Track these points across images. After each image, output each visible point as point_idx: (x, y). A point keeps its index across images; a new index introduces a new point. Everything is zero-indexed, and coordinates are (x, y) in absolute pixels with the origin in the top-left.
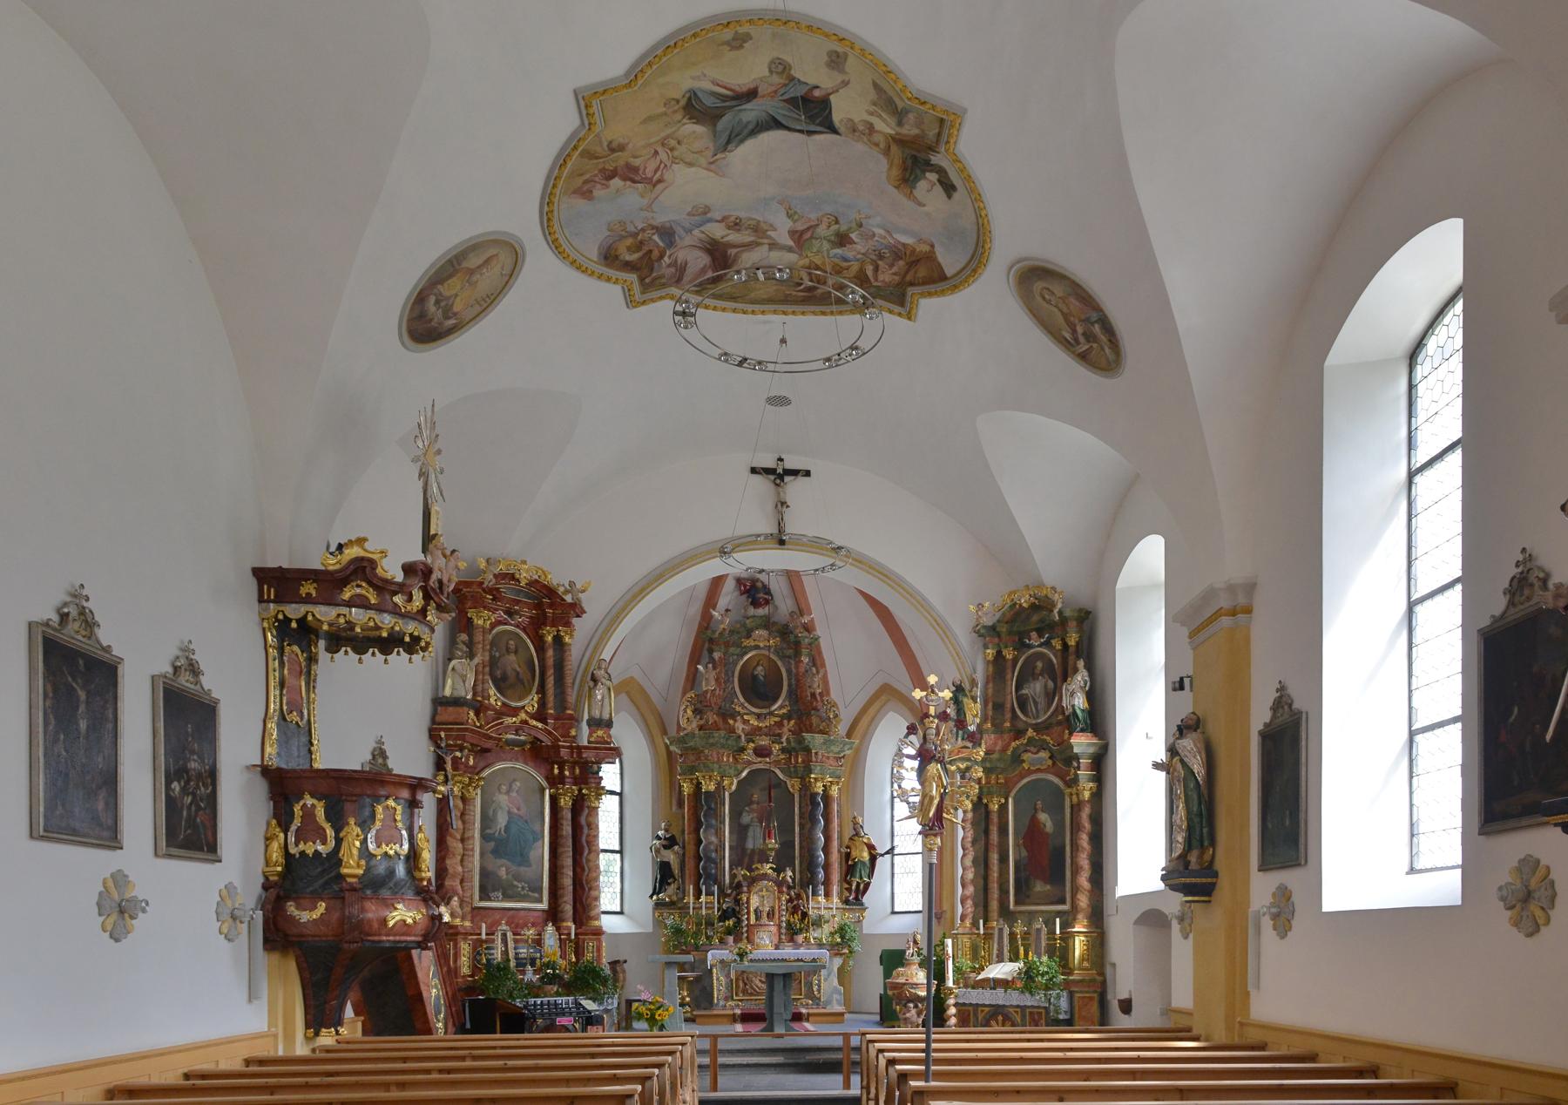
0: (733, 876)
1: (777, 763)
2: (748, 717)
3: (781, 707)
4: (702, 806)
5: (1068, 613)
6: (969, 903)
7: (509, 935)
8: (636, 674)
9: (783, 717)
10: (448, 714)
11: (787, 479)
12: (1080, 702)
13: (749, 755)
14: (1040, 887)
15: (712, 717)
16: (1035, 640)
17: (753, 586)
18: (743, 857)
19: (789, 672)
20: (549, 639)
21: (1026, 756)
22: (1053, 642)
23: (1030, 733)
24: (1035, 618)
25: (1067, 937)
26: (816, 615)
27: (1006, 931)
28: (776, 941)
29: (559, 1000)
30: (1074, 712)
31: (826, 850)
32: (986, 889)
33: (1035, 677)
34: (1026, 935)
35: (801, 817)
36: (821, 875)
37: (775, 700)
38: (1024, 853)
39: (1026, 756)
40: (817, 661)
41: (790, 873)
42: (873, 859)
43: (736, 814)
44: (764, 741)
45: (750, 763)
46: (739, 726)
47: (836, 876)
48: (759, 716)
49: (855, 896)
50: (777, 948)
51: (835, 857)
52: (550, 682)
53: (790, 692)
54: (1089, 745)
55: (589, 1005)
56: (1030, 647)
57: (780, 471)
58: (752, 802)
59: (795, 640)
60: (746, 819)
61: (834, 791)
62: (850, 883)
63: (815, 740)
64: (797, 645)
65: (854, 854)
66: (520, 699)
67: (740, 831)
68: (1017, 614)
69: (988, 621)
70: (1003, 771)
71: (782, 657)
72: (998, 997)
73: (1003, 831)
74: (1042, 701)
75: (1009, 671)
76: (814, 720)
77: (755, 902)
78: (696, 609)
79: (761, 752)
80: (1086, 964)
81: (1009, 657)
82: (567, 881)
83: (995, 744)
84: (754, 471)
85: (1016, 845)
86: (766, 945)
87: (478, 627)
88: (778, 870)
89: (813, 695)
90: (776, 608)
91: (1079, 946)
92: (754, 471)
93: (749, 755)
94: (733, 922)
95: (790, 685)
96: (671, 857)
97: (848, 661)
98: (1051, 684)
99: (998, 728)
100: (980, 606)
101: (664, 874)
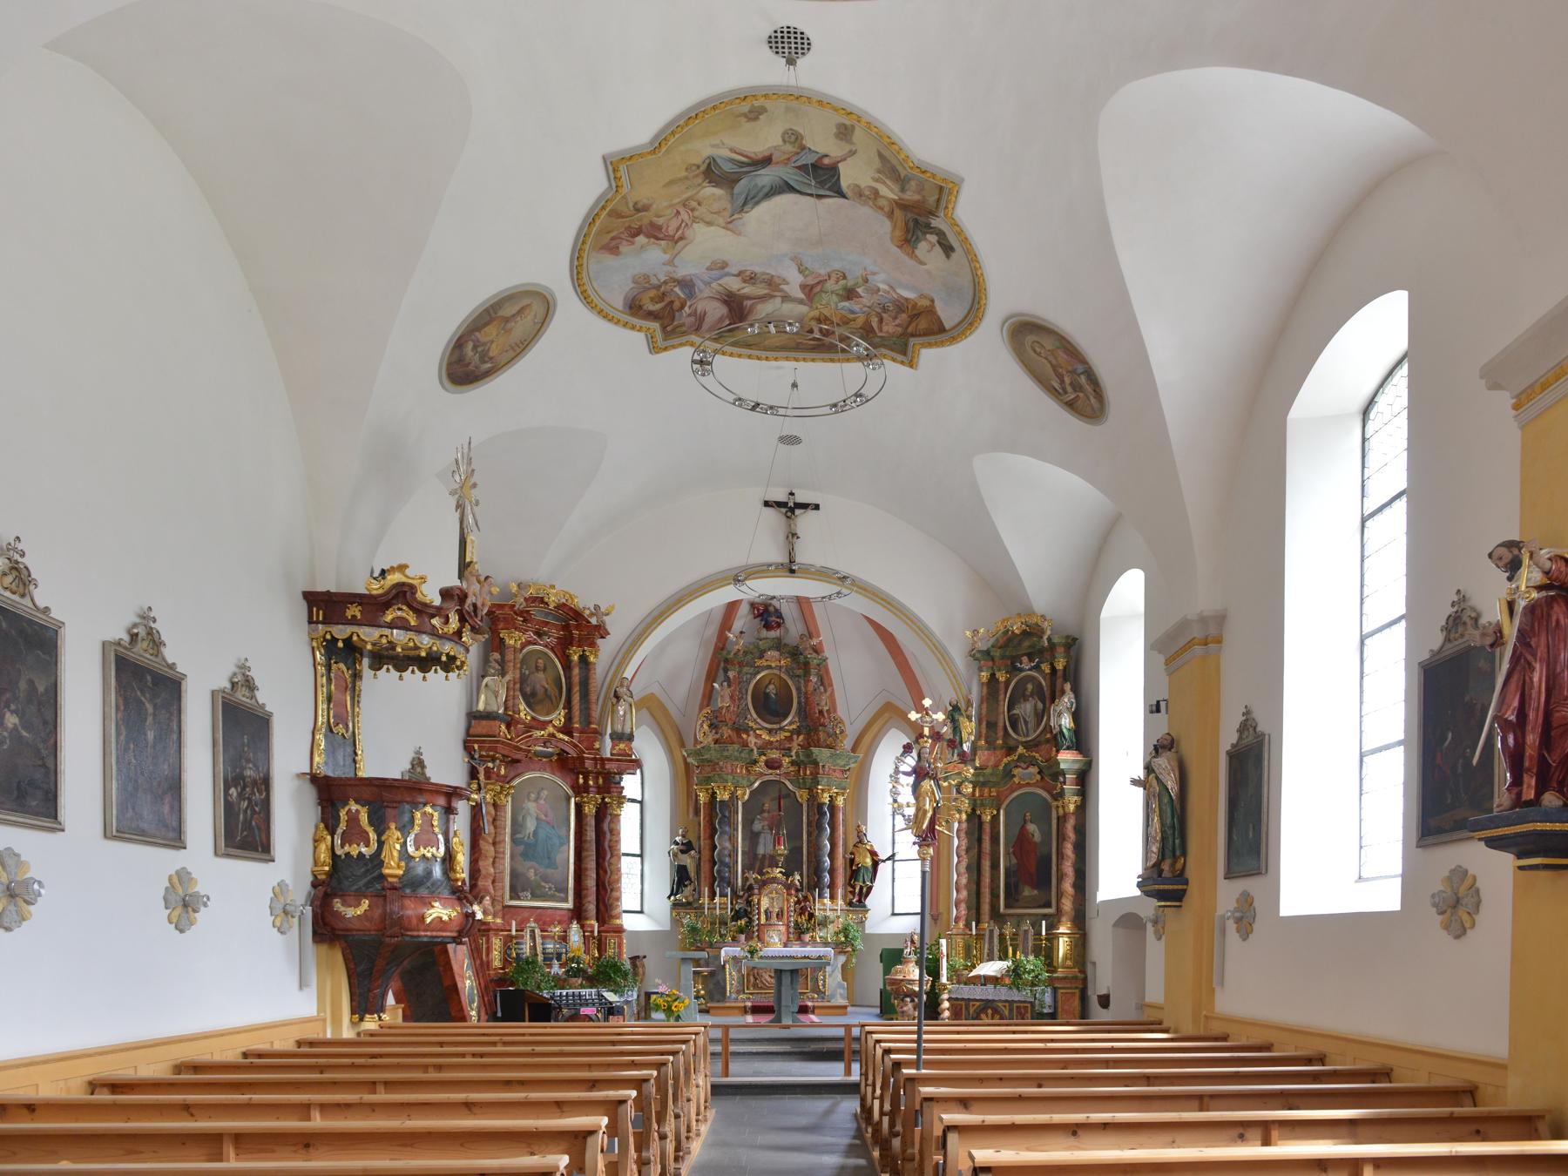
5: (1056, 640)
6: (963, 906)
12: (1066, 722)
14: (1027, 892)
16: (1025, 663)
21: (1016, 771)
23: (1021, 750)
25: (1052, 938)
27: (996, 932)
28: (784, 939)
30: (1061, 732)
31: (832, 855)
32: (978, 893)
34: (1014, 936)
36: (827, 879)
38: (1014, 861)
39: (1016, 771)
42: (875, 864)
47: (840, 880)
49: (858, 899)
50: (785, 946)
51: (840, 862)
52: (576, 698)
66: (548, 714)
68: (1010, 640)
70: (996, 784)
72: (989, 993)
74: (1032, 721)
77: (765, 903)
80: (1069, 963)
81: (1002, 679)
82: (591, 882)
85: (1007, 853)
88: (787, 874)
91: (1063, 946)
98: (1040, 705)
99: (991, 744)
100: (975, 632)
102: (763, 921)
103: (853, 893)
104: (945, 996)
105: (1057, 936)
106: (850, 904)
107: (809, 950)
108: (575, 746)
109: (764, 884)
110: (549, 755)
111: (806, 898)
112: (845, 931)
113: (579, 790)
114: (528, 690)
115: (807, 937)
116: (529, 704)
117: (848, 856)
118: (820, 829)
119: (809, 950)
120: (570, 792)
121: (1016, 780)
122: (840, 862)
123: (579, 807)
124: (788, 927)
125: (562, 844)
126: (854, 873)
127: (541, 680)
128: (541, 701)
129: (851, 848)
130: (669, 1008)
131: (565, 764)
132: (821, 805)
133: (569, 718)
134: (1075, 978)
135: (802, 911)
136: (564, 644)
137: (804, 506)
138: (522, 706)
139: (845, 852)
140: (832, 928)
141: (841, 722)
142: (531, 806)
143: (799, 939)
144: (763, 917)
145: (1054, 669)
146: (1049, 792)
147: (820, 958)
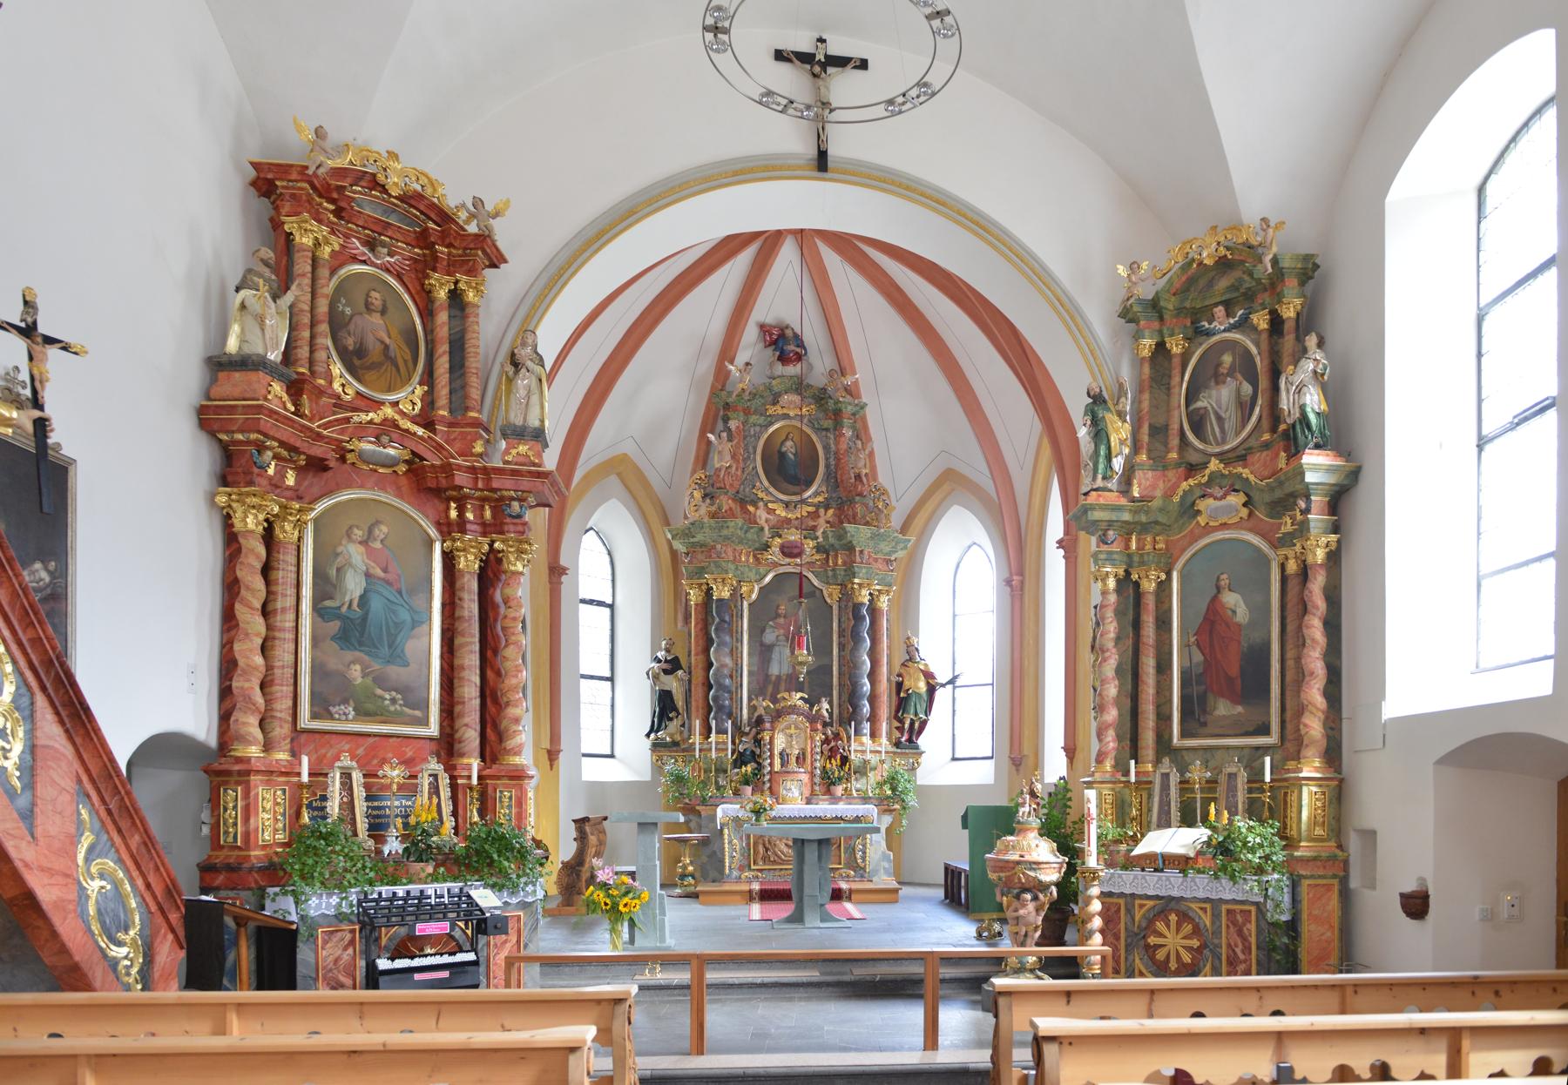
0: (752, 709)
1: (811, 564)
2: (772, 507)
3: (816, 494)
4: (711, 619)
5: (1286, 263)
6: (1110, 735)
7: (357, 777)
8: (629, 448)
9: (817, 506)
10: (237, 381)
11: (830, 70)
12: (1313, 400)
13: (774, 554)
14: (1223, 709)
15: (726, 503)
16: (1220, 322)
17: (782, 336)
18: (765, 685)
19: (826, 448)
20: (442, 294)
21: (1202, 505)
22: (1255, 318)
23: (1214, 465)
24: (1223, 283)
26: (861, 375)
27: (1174, 779)
28: (807, 793)
29: (430, 889)
30: (1304, 419)
31: (872, 676)
32: (1135, 713)
33: (1218, 379)
35: (840, 635)
36: (866, 709)
37: (809, 484)
38: (1198, 657)
40: (862, 434)
41: (826, 706)
42: (931, 690)
43: (757, 631)
44: (793, 536)
45: (776, 565)
46: (762, 515)
48: (787, 505)
49: (908, 737)
50: (808, 802)
51: (884, 686)
52: (443, 364)
53: (828, 475)
54: (1330, 470)
55: (486, 898)
56: (1209, 334)
57: (820, 57)
58: (778, 616)
59: (834, 407)
60: (769, 637)
61: (883, 603)
62: (901, 721)
63: (859, 534)
64: (837, 414)
65: (907, 684)
66: (389, 390)
67: (763, 652)
68: (1191, 281)
69: (1146, 291)
70: (1166, 528)
71: (818, 430)
72: (1171, 884)
73: (1163, 623)
74: (1231, 417)
75: (1176, 372)
76: (859, 509)
77: (780, 742)
78: (707, 366)
79: (790, 551)
80: (1319, 831)
81: (1176, 350)
82: (470, 690)
83: (1154, 487)
84: (780, 56)
85: (1184, 645)
86: (794, 800)
87: (303, 248)
88: (811, 702)
89: (858, 477)
90: (811, 367)
91: (1308, 802)
92: (780, 56)
93: (774, 554)
94: (751, 765)
95: (827, 466)
96: (673, 684)
97: (903, 427)
98: (1247, 389)
99: (1159, 463)
100: (1133, 267)
101: (665, 707)
102: (777, 767)
103: (901, 729)
104: (1095, 891)
105: (1299, 783)
106: (897, 744)
107: (842, 808)
108: (439, 447)
109: (778, 715)
110: (391, 463)
111: (837, 736)
112: (892, 781)
113: (447, 529)
114: (350, 343)
115: (839, 790)
116: (351, 368)
117: (895, 679)
118: (856, 638)
119: (842, 808)
120: (433, 532)
121: (1202, 520)
122: (884, 686)
123: (449, 559)
124: (812, 775)
125: (415, 624)
126: (902, 702)
127: (375, 329)
128: (374, 366)
129: (897, 669)
130: (615, 907)
131: (426, 481)
132: (857, 607)
133: (429, 401)
134: (1333, 858)
135: (833, 753)
136: (425, 265)
137: (842, 62)
138: (337, 369)
139: (890, 672)
140: (873, 777)
141: (885, 492)
142: (355, 553)
143: (828, 792)
144: (777, 761)
145: (1276, 322)
146: (1263, 536)
147: (857, 819)
